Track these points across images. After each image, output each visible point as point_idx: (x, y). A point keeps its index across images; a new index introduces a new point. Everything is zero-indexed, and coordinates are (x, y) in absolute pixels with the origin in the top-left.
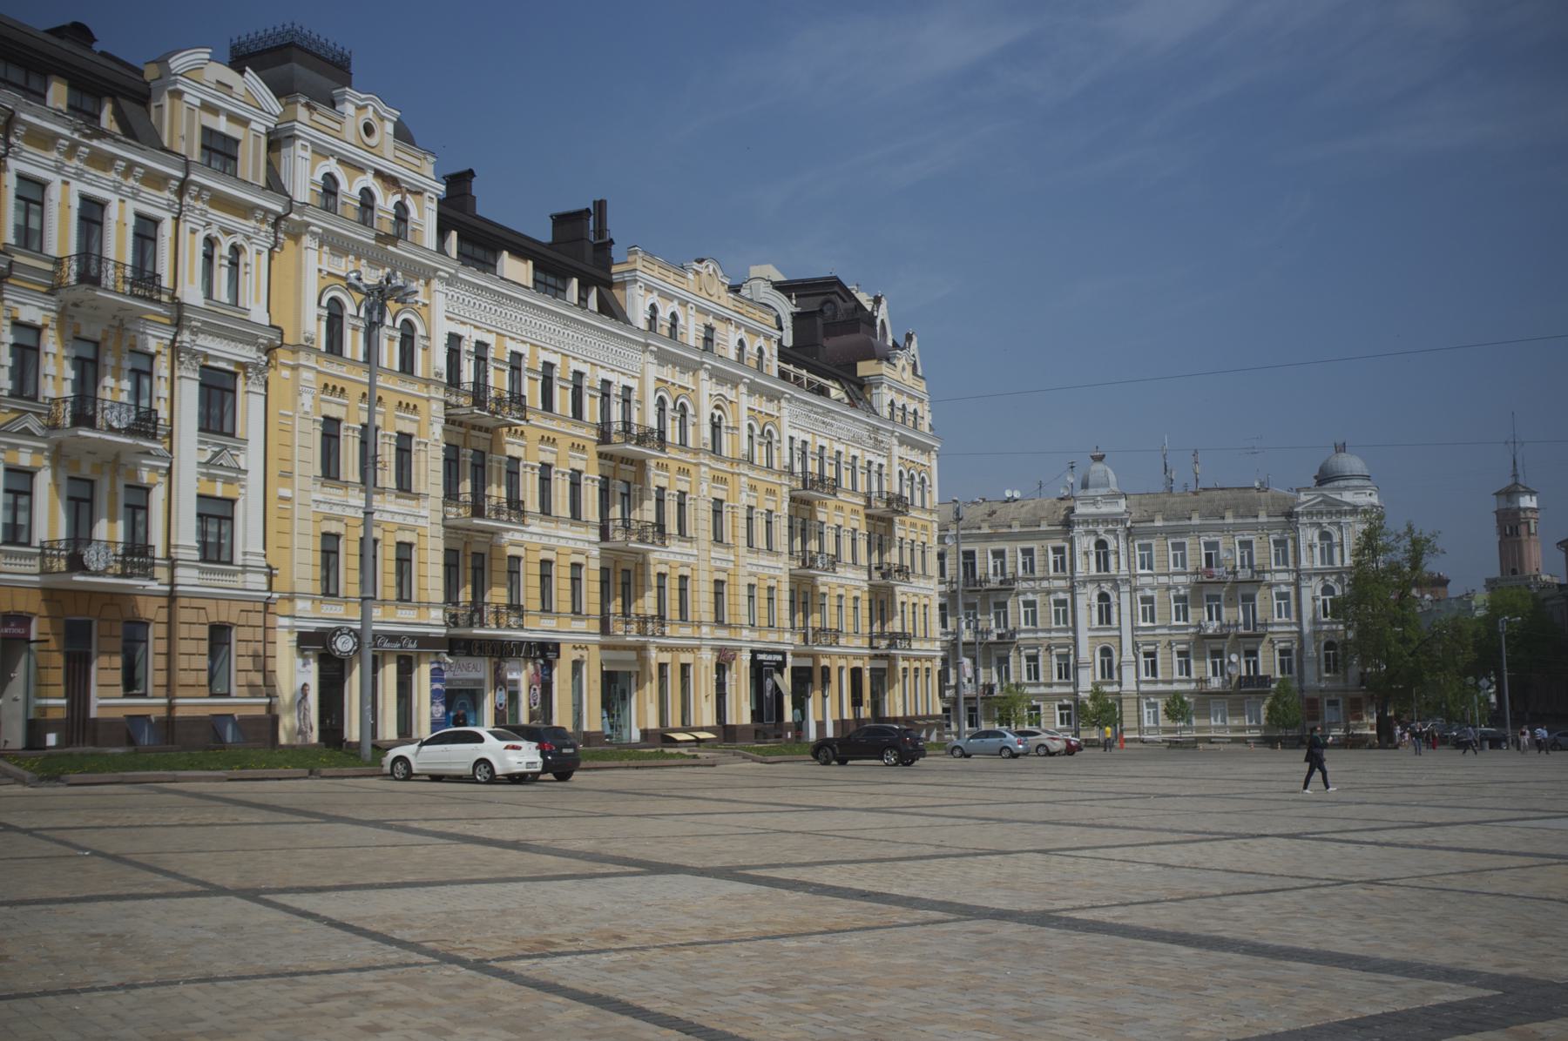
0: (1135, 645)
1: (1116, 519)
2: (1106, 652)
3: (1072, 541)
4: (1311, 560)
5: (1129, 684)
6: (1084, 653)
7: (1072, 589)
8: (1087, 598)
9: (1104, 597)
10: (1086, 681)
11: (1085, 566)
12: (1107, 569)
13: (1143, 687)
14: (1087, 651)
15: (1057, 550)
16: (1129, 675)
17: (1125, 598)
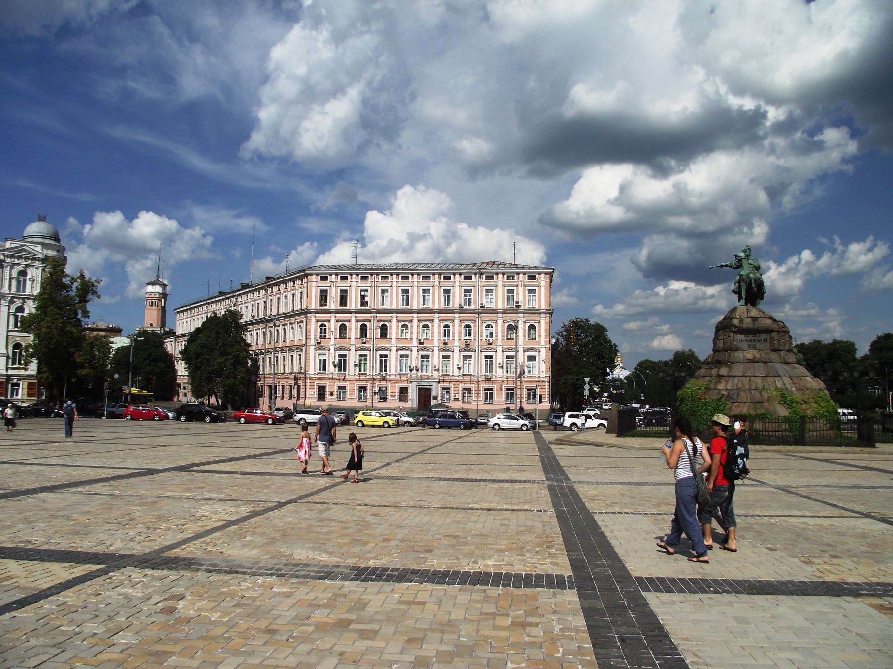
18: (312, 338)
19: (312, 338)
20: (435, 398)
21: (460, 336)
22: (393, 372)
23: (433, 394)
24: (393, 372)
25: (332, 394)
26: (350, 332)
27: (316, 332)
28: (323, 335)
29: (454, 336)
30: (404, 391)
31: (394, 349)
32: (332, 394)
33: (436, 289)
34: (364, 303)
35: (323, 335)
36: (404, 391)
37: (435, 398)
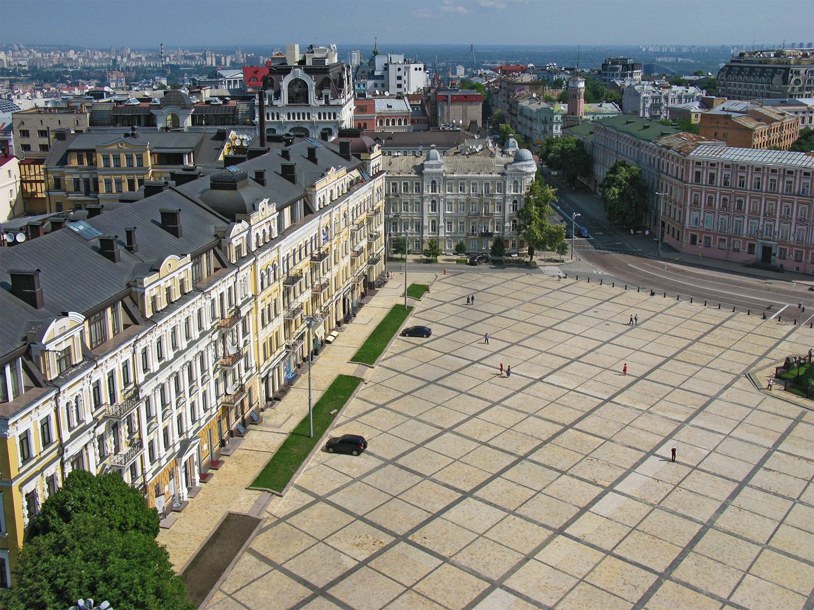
0: (445, 220)
1: (441, 174)
2: (433, 222)
3: (423, 180)
4: (510, 192)
5: (442, 235)
6: (426, 224)
7: (422, 199)
8: (427, 204)
9: (434, 202)
10: (427, 234)
11: (427, 192)
12: (435, 192)
13: (447, 235)
14: (427, 222)
15: (416, 184)
16: (442, 231)
17: (442, 203)
18: (689, 202)
19: (689, 202)
20: (774, 255)
21: (797, 215)
22: (745, 232)
23: (773, 252)
24: (745, 232)
25: (700, 242)
26: (715, 202)
27: (691, 199)
28: (696, 203)
29: (792, 215)
30: (751, 247)
31: (746, 217)
32: (700, 242)
33: (781, 179)
34: (726, 183)
35: (696, 203)
36: (751, 247)
37: (774, 255)
